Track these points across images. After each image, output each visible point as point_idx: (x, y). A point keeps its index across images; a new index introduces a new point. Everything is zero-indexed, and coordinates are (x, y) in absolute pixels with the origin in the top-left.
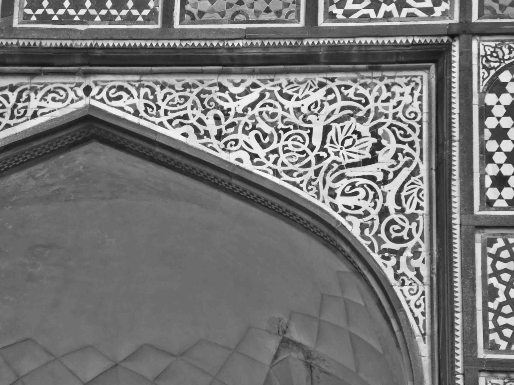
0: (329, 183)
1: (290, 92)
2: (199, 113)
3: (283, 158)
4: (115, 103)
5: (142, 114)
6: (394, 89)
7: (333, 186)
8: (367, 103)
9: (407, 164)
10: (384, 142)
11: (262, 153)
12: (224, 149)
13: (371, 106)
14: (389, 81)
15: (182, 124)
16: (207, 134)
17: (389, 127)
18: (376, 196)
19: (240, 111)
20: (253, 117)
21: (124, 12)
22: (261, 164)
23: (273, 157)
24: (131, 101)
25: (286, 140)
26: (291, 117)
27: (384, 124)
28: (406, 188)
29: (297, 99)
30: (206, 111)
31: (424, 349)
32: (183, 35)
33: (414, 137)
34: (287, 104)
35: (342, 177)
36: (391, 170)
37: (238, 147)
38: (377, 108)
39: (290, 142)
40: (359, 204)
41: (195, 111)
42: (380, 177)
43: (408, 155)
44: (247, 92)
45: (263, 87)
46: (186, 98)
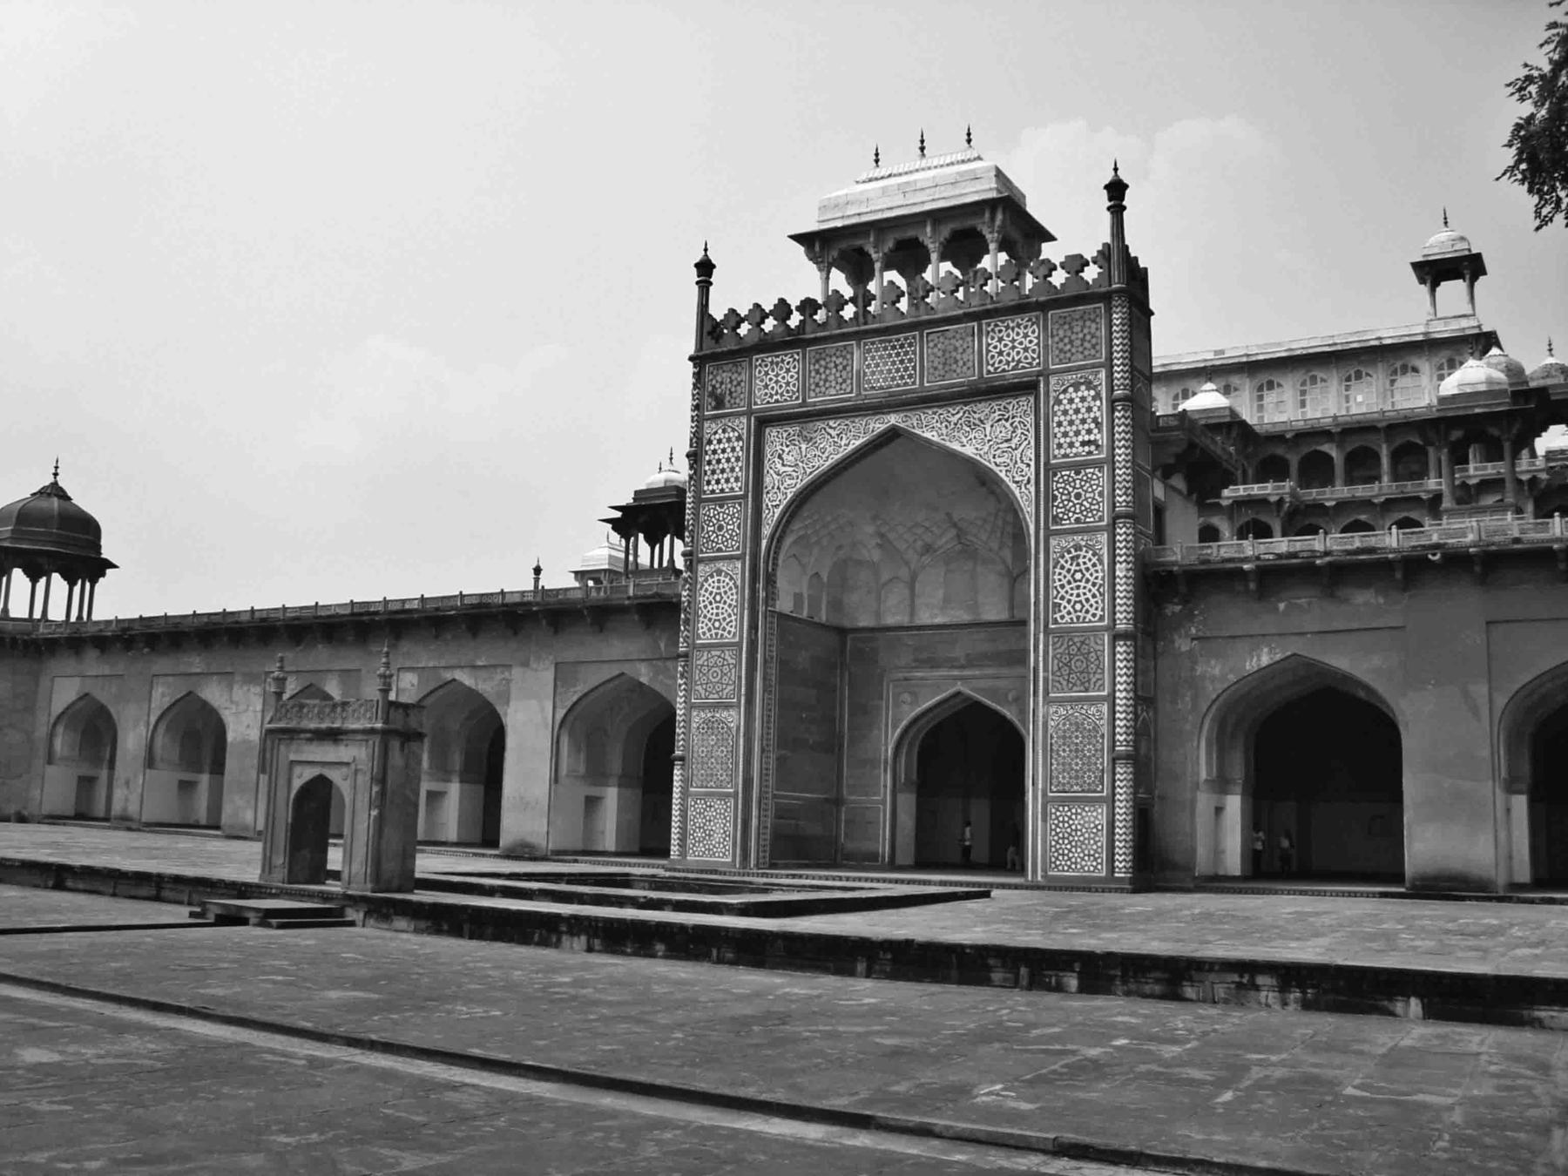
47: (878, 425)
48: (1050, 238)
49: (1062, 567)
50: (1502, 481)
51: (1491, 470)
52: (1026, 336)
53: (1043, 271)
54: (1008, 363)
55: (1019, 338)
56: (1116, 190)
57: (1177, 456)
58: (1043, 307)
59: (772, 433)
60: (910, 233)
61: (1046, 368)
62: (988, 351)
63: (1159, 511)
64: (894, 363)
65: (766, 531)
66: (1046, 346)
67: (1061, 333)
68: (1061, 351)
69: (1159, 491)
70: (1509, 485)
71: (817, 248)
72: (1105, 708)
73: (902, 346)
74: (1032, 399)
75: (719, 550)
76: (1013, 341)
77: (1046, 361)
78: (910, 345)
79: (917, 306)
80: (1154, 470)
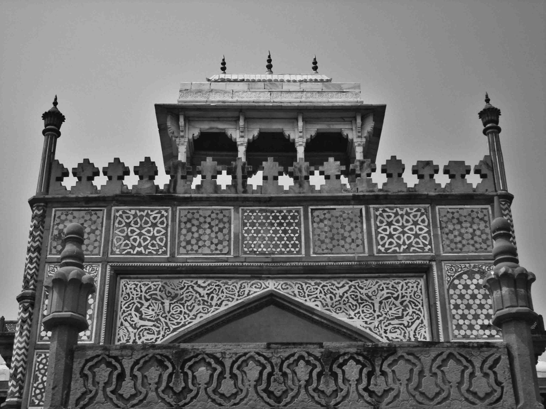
0: (383, 327)
1: (362, 286)
2: (323, 296)
3: (362, 315)
4: (285, 291)
5: (298, 296)
6: (409, 284)
7: (386, 328)
8: (398, 291)
9: (418, 318)
10: (407, 309)
11: (352, 313)
12: (335, 312)
13: (400, 292)
14: (406, 281)
15: (315, 301)
16: (327, 305)
17: (409, 302)
18: (405, 333)
19: (341, 294)
20: (347, 297)
21: (288, 249)
22: (352, 318)
23: (358, 315)
24: (292, 290)
25: (363, 307)
26: (364, 297)
27: (405, 300)
28: (418, 329)
29: (366, 289)
30: (325, 295)
33: (420, 306)
34: (362, 291)
35: (390, 324)
36: (410, 321)
37: (341, 311)
38: (402, 293)
39: (365, 309)
40: (397, 336)
41: (321, 295)
42: (406, 324)
43: (418, 314)
44: (343, 286)
45: (351, 283)
46: (317, 289)
52: (415, 223)
54: (399, 246)
55: (409, 225)
56: (490, 117)
59: (128, 286)
60: (275, 127)
61: (438, 255)
62: (377, 233)
64: (276, 232)
66: (436, 236)
67: (451, 227)
68: (452, 241)
73: (285, 217)
74: (422, 282)
76: (403, 227)
77: (437, 248)
78: (294, 217)
79: (301, 186)
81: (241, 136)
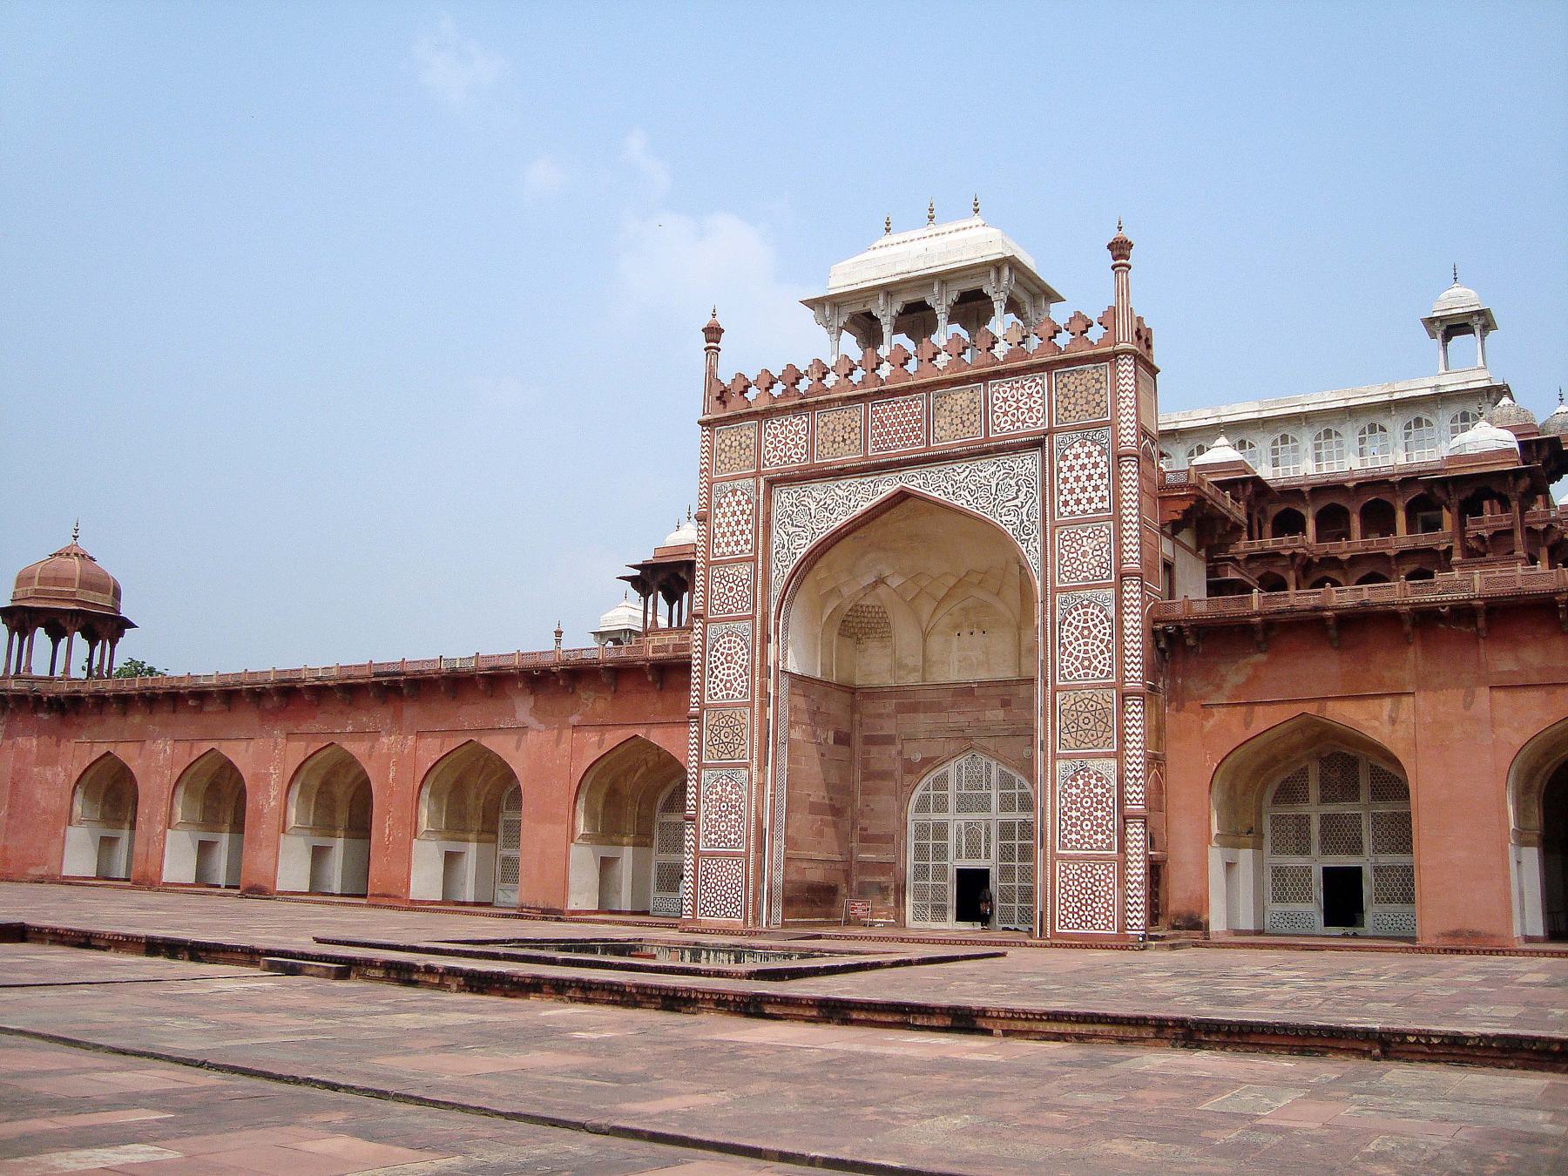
31: (1038, 584)
32: (934, 449)
47: (887, 486)
48: (1052, 297)
49: (1070, 624)
50: (1510, 533)
51: (1504, 521)
53: (1046, 330)
57: (1186, 513)
58: (1046, 367)
63: (1168, 567)
65: (776, 592)
69: (1166, 548)
70: (1518, 536)
71: (827, 313)
72: (1113, 763)
75: (730, 611)
76: (1018, 401)
80: (1163, 525)
81: (886, 314)
